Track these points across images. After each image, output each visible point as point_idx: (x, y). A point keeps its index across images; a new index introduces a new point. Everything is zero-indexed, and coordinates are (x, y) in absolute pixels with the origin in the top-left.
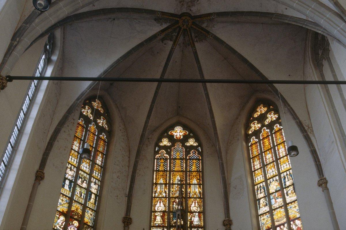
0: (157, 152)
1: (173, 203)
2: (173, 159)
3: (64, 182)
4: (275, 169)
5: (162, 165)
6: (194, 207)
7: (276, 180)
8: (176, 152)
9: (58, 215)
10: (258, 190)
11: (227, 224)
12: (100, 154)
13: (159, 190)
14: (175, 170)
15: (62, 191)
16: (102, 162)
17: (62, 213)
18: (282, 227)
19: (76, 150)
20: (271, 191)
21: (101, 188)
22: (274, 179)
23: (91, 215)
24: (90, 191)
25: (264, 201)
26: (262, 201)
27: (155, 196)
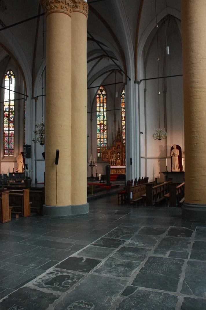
17: (99, 125)
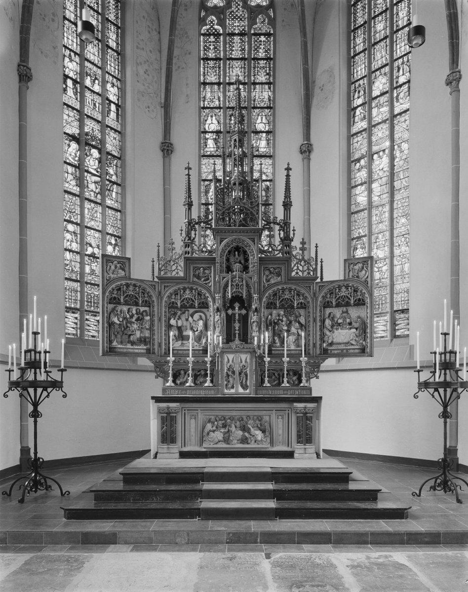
0: (202, 21)
1: (230, 116)
2: (229, 34)
3: (65, 82)
4: (386, 53)
5: (212, 47)
6: (261, 124)
7: (385, 74)
8: (233, 19)
9: (66, 139)
10: (355, 91)
11: (305, 151)
12: (112, 27)
13: (209, 95)
14: (233, 56)
15: (65, 99)
16: (118, 44)
17: (73, 138)
18: (381, 153)
19: (72, 20)
20: (376, 93)
21: (122, 91)
22: (383, 70)
23: (115, 139)
24: (108, 99)
25: (362, 111)
26: (358, 112)
27: (204, 104)
